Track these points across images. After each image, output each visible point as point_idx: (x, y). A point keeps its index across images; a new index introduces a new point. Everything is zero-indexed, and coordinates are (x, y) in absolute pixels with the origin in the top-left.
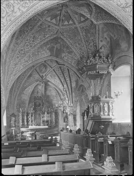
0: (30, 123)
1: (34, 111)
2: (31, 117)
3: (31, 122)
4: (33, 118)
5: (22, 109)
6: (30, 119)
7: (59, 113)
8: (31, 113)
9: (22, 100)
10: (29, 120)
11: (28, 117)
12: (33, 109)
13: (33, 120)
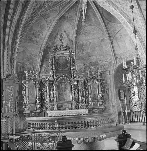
0: (47, 104)
1: (55, 77)
2: (50, 90)
3: (50, 101)
4: (54, 93)
5: (29, 72)
6: (46, 95)
7: (109, 82)
8: (50, 81)
9: (29, 55)
10: (46, 98)
11: (42, 91)
12: (53, 73)
13: (54, 97)
